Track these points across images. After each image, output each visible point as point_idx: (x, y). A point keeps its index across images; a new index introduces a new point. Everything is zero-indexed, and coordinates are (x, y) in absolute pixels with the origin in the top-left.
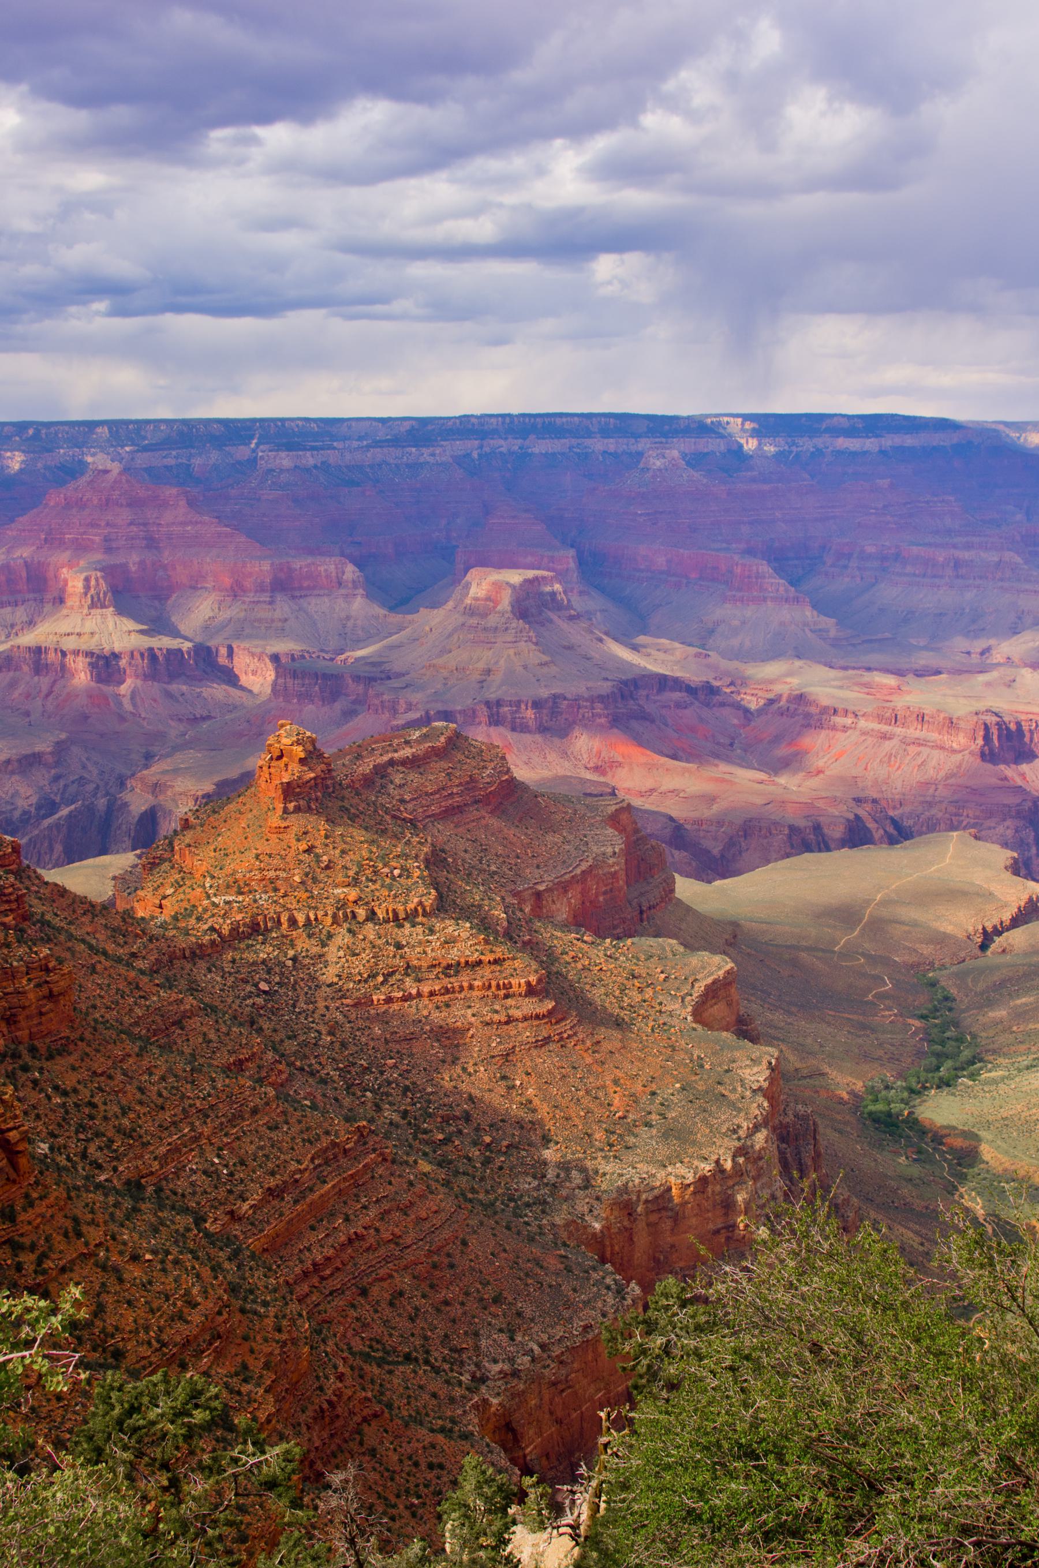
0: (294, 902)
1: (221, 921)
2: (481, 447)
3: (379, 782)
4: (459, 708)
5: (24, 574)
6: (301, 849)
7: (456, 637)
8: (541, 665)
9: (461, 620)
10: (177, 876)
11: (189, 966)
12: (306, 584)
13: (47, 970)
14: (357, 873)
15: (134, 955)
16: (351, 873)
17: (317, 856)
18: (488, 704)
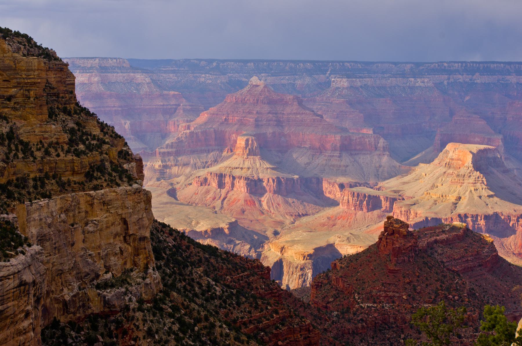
0: (403, 309)
1: (366, 316)
2: (449, 79)
3: (429, 252)
4: (444, 217)
5: (213, 136)
6: (406, 281)
7: (440, 179)
8: (490, 196)
9: (444, 170)
10: (335, 292)
11: (351, 338)
12: (358, 147)
13: (309, 331)
14: (436, 297)
15: (325, 330)
16: (433, 297)
17: (414, 285)
18: (459, 216)
